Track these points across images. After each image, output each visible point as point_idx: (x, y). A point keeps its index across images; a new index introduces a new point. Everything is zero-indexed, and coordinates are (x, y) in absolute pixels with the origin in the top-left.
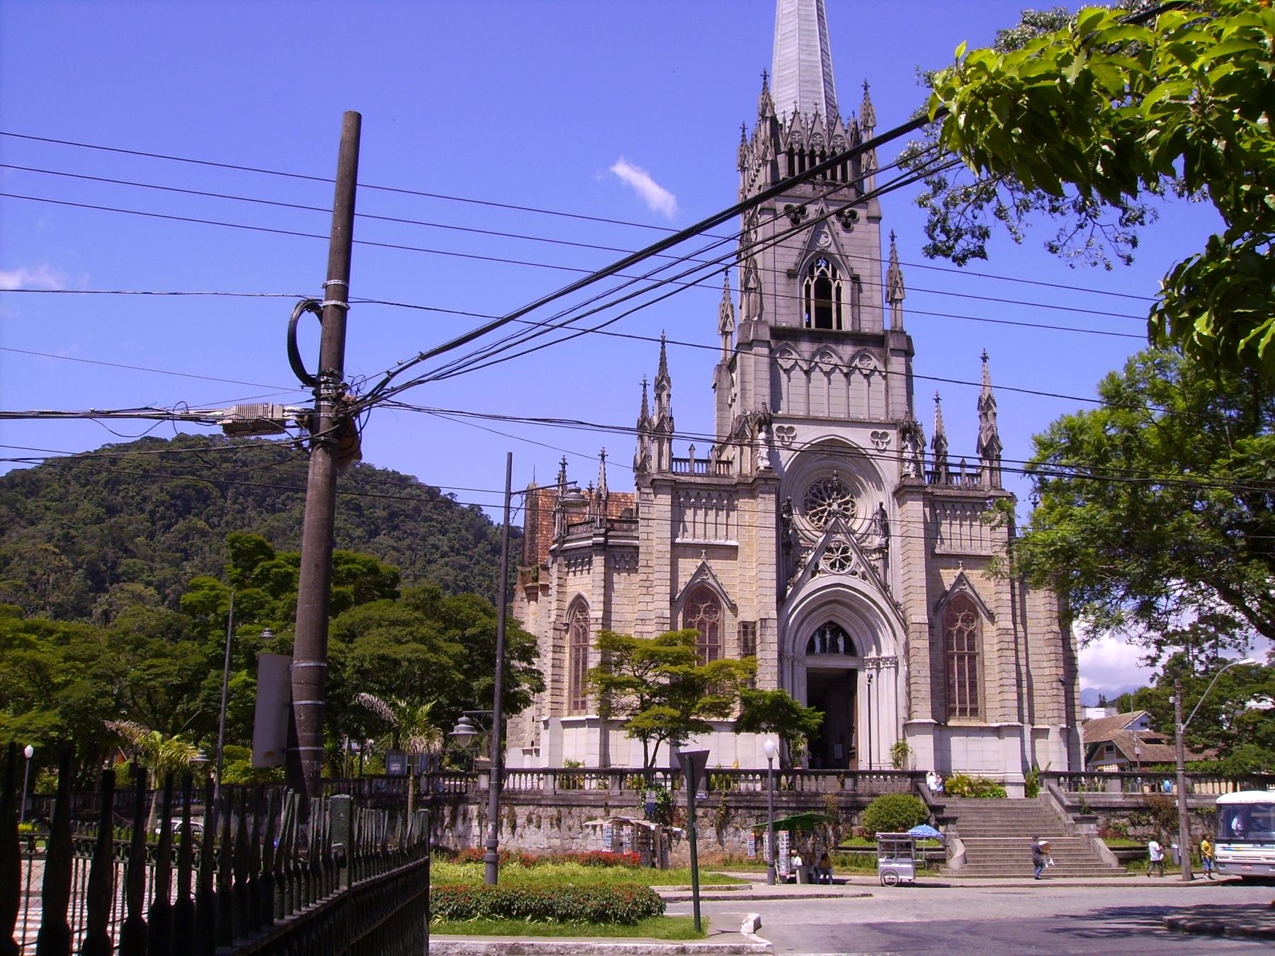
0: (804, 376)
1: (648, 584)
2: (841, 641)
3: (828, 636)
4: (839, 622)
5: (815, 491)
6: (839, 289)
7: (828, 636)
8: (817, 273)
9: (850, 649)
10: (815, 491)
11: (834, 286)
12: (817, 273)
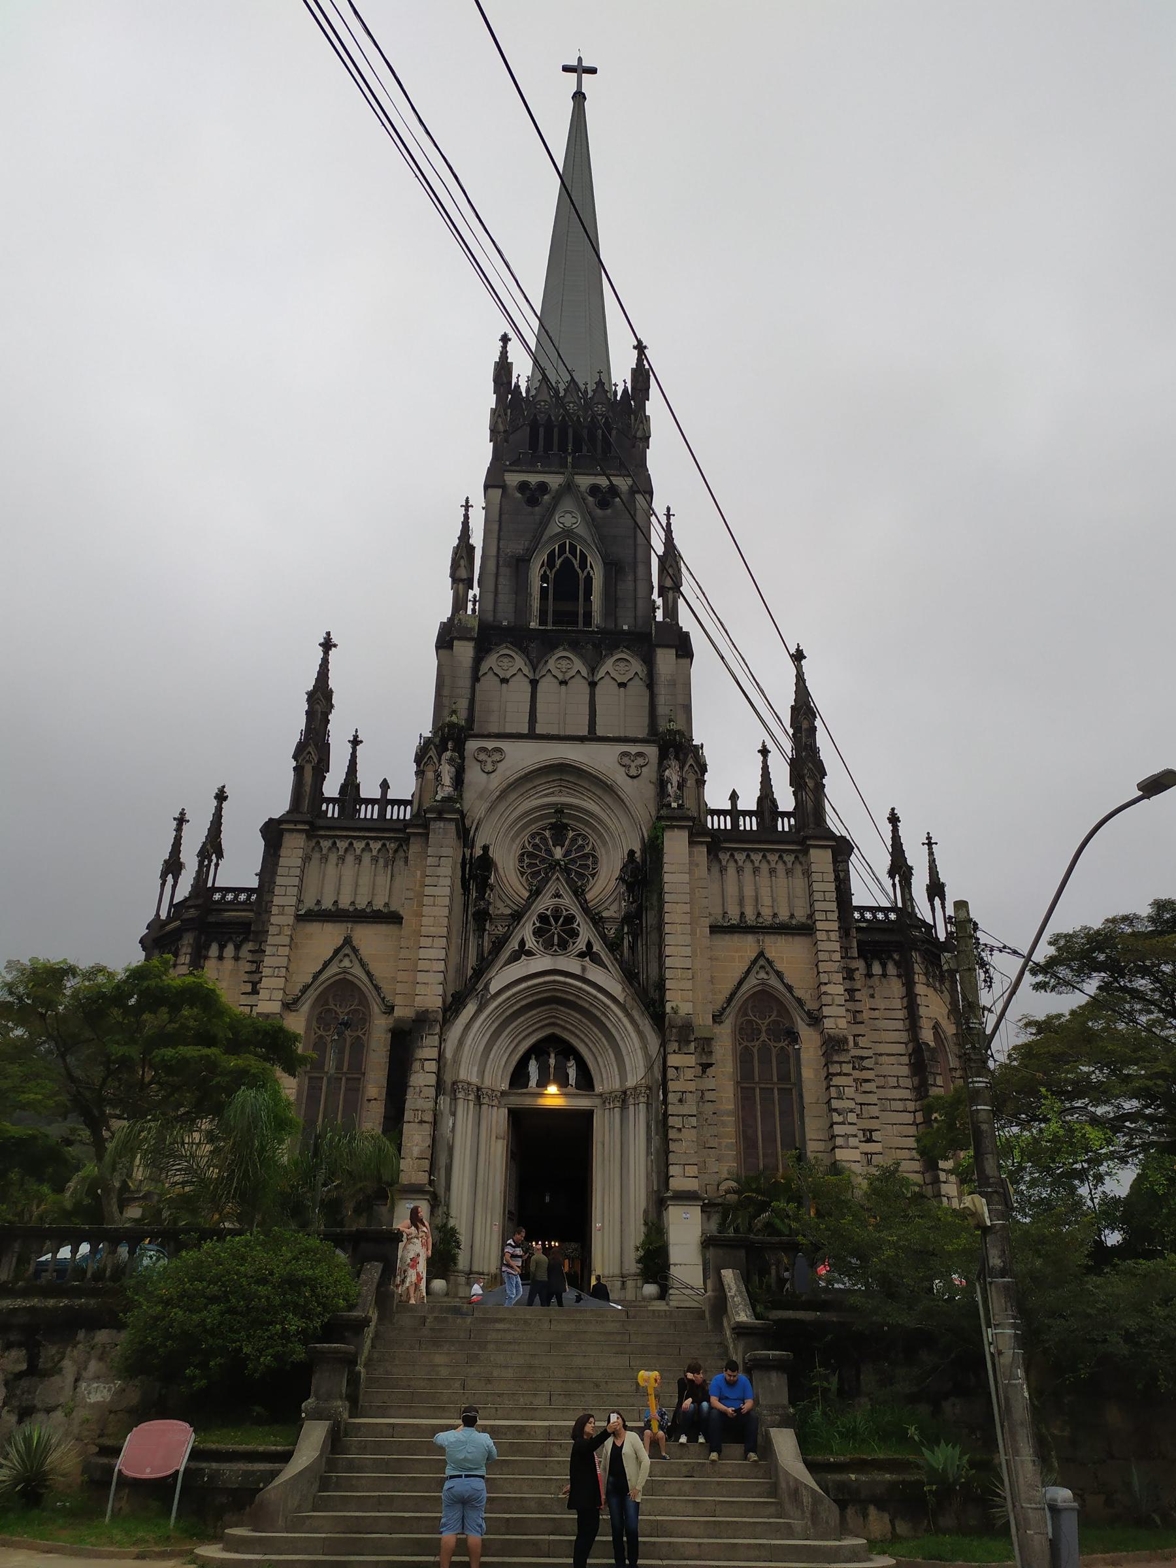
1: (256, 977)
2: (572, 1073)
3: (552, 1061)
4: (566, 1036)
5: (537, 841)
6: (589, 580)
7: (552, 1061)
8: (558, 562)
9: (586, 1082)
10: (537, 841)
11: (582, 576)
12: (558, 562)
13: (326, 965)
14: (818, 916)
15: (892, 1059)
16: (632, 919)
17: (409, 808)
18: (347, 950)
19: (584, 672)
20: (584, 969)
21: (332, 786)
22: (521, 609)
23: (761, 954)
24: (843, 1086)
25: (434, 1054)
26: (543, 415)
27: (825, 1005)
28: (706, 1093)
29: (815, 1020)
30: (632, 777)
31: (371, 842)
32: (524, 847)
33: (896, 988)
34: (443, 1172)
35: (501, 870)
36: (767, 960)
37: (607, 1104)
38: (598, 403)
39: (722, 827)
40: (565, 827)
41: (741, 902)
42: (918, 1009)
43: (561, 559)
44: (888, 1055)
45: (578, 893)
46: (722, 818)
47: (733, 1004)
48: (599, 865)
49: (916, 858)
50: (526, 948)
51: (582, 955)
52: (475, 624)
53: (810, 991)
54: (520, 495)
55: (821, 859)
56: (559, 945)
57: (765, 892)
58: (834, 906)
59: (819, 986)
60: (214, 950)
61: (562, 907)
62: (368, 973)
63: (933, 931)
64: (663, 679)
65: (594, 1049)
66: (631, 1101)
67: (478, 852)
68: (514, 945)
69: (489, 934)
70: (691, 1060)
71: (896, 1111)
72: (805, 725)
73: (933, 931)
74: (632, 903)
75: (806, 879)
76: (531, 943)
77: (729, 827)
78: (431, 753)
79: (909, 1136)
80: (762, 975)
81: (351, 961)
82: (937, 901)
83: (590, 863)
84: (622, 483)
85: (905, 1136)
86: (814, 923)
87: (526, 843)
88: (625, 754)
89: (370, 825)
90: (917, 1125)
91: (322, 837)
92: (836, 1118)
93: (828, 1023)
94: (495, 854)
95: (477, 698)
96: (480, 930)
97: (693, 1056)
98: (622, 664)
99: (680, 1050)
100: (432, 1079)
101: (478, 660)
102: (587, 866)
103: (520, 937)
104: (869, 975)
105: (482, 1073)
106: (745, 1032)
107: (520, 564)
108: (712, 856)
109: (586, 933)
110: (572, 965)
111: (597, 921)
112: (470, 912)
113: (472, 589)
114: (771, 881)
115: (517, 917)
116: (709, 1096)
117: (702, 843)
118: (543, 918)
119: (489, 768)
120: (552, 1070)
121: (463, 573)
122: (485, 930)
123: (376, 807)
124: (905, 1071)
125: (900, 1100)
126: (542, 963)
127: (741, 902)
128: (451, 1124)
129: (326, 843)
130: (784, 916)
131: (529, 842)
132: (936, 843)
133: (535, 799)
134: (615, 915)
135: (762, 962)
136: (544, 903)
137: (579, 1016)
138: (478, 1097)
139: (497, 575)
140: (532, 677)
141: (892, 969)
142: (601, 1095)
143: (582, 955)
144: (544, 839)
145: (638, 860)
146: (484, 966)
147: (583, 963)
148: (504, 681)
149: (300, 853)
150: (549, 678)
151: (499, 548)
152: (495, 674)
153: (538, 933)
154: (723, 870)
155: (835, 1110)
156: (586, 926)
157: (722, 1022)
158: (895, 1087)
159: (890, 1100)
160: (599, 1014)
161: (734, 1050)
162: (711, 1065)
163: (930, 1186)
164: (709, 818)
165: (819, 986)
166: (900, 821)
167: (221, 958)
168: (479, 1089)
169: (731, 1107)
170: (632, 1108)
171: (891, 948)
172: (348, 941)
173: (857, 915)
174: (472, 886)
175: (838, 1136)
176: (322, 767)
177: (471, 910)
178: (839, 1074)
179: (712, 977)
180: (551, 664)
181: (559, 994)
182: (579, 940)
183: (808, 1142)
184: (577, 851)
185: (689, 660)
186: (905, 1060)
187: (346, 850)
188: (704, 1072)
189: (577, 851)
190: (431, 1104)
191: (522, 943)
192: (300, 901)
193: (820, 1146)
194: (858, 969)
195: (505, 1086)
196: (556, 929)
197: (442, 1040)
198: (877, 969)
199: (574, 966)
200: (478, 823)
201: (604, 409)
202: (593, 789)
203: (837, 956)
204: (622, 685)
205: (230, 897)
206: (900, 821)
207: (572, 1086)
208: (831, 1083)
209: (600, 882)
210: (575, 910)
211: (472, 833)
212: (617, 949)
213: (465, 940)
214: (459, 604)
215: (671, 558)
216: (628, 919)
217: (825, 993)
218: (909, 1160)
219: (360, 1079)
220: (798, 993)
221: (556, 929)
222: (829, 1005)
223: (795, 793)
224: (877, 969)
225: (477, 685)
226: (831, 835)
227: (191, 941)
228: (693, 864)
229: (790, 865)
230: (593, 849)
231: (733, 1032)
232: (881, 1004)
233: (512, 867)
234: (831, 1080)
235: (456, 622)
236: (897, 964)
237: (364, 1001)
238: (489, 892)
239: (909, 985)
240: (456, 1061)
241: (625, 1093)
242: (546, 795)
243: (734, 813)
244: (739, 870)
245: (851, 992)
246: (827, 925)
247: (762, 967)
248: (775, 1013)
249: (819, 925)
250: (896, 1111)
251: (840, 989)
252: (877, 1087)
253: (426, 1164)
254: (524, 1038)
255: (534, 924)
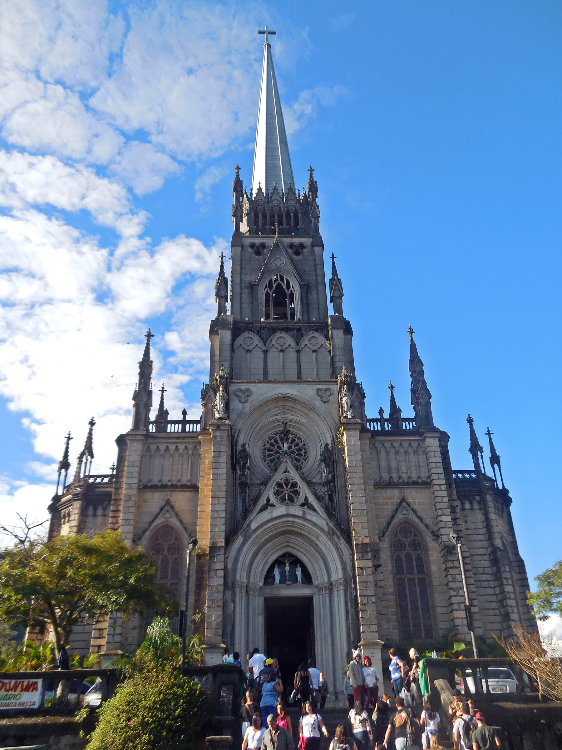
0: (262, 355)
2: (299, 573)
3: (287, 568)
4: (295, 552)
5: (272, 441)
6: (292, 295)
7: (287, 568)
8: (274, 286)
9: (308, 579)
10: (272, 441)
11: (288, 293)
12: (274, 286)
13: (156, 516)
14: (434, 477)
15: (479, 558)
16: (331, 482)
17: (199, 425)
18: (167, 508)
19: (293, 344)
20: (304, 513)
21: (153, 416)
22: (254, 312)
23: (403, 500)
24: (455, 575)
25: (222, 566)
26: (260, 207)
27: (441, 528)
28: (378, 583)
29: (436, 536)
30: (324, 402)
31: (179, 445)
32: (265, 445)
33: (479, 516)
34: (229, 636)
35: (253, 458)
36: (407, 503)
37: (321, 592)
38: (290, 200)
39: (376, 429)
40: (288, 432)
41: (389, 470)
42: (492, 528)
43: (276, 284)
44: (477, 555)
45: (298, 468)
46: (375, 423)
47: (390, 529)
48: (308, 452)
49: (483, 442)
50: (271, 502)
51: (303, 505)
52: (231, 320)
53: (432, 521)
54: (251, 250)
55: (432, 443)
56: (289, 500)
57: (403, 464)
58: (442, 471)
59: (437, 517)
60: (90, 511)
61: (290, 478)
62: (181, 521)
63: (495, 483)
64: (337, 347)
65: (312, 560)
66: (335, 589)
67: (239, 448)
68: (262, 502)
69: (248, 495)
70: (370, 563)
71: (484, 588)
72: (418, 370)
73: (495, 483)
74: (329, 474)
75: (425, 456)
76: (273, 500)
77: (379, 429)
78: (210, 394)
79: (492, 602)
80: (405, 512)
81: (170, 514)
82: (496, 466)
83: (303, 452)
84: (307, 241)
85: (490, 602)
86: (432, 481)
87: (266, 442)
88: (319, 390)
89: (177, 435)
90: (496, 595)
91: (151, 443)
92: (453, 593)
93: (444, 538)
94: (250, 449)
95: (234, 362)
96: (243, 492)
97: (371, 561)
98: (314, 340)
99: (363, 557)
100: (221, 581)
101: (233, 340)
102: (300, 455)
103: (266, 497)
104: (463, 509)
105: (248, 577)
106: (397, 546)
107: (252, 287)
108: (372, 446)
109: (305, 491)
110: (296, 510)
111: (310, 484)
112: (237, 483)
113: (227, 302)
114: (406, 458)
115: (265, 483)
116: (380, 584)
117: (366, 438)
118: (279, 485)
119: (243, 400)
120: (287, 573)
121: (222, 293)
122: (246, 493)
123: (180, 425)
124: (487, 564)
125: (486, 581)
126: (280, 510)
127: (389, 470)
128: (232, 608)
129: (153, 446)
130: (414, 477)
131: (268, 442)
132: (493, 434)
133: (271, 417)
134: (319, 481)
135: (404, 504)
136: (279, 476)
137: (302, 541)
138: (247, 591)
139: (241, 293)
140: (264, 348)
141: (476, 506)
142: (317, 586)
143: (303, 505)
144: (276, 441)
145: (330, 449)
146: (247, 512)
147: (304, 510)
148: (248, 351)
149: (139, 453)
150: (274, 349)
151: (241, 279)
152: (244, 348)
153: (277, 493)
154: (378, 453)
155: (452, 589)
156: (304, 488)
157: (384, 541)
158: (482, 574)
159: (480, 581)
160: (313, 538)
161: (392, 557)
162: (379, 566)
163: (507, 630)
164: (368, 423)
165: (437, 517)
166: (473, 422)
167: (95, 515)
168: (247, 586)
169: (392, 590)
170: (336, 593)
171: (475, 494)
172: (168, 502)
173: (454, 476)
174: (238, 467)
175: (455, 603)
176: (148, 405)
177: (238, 482)
178: (452, 568)
179: (377, 515)
180: (274, 342)
181: (290, 528)
182: (301, 496)
183: (437, 608)
184: (295, 446)
185: (351, 336)
186: (487, 557)
187: (165, 451)
188: (376, 570)
189: (295, 446)
190: (221, 596)
191: (268, 500)
192: (140, 481)
193: (445, 610)
194: (457, 506)
195: (261, 584)
196: (286, 491)
197: (226, 558)
198: (467, 506)
199: (298, 511)
200: (239, 431)
201: (294, 203)
202: (303, 409)
203: (446, 499)
204: (314, 351)
205: (99, 480)
206: (473, 422)
207: (300, 582)
208: (449, 573)
209: (309, 463)
210: (297, 479)
211: (236, 437)
212: (323, 500)
213: (235, 499)
214: (222, 309)
215: (336, 282)
216: (327, 483)
217: (441, 521)
218: (494, 615)
219: (177, 584)
220: (427, 522)
221: (286, 491)
222: (443, 528)
223: (414, 408)
224: (467, 506)
225: (234, 355)
226: (436, 430)
227: (78, 506)
228: (363, 450)
229: (415, 449)
230: (304, 444)
231: (390, 546)
232: (471, 526)
233: (259, 456)
234: (448, 571)
235: (220, 320)
236: (479, 502)
237: (178, 538)
238: (247, 471)
239: (486, 514)
240: (234, 570)
241: (331, 584)
242: (276, 415)
243: (381, 420)
244: (387, 453)
245: (454, 520)
246: (439, 481)
247: (405, 508)
248: (413, 533)
249: (435, 482)
250: (484, 588)
251: (449, 518)
252: (473, 574)
253: (220, 631)
254: (271, 555)
255: (274, 488)
